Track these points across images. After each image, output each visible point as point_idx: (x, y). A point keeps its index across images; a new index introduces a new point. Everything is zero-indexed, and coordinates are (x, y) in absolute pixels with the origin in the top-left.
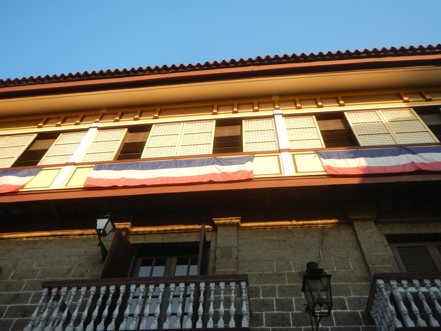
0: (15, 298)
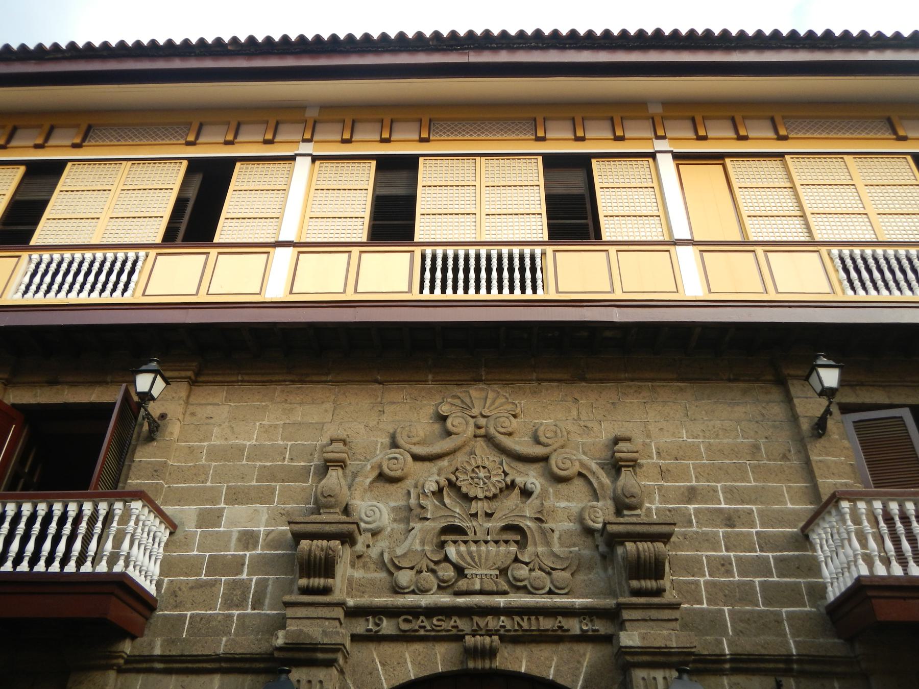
0: (691, 495)
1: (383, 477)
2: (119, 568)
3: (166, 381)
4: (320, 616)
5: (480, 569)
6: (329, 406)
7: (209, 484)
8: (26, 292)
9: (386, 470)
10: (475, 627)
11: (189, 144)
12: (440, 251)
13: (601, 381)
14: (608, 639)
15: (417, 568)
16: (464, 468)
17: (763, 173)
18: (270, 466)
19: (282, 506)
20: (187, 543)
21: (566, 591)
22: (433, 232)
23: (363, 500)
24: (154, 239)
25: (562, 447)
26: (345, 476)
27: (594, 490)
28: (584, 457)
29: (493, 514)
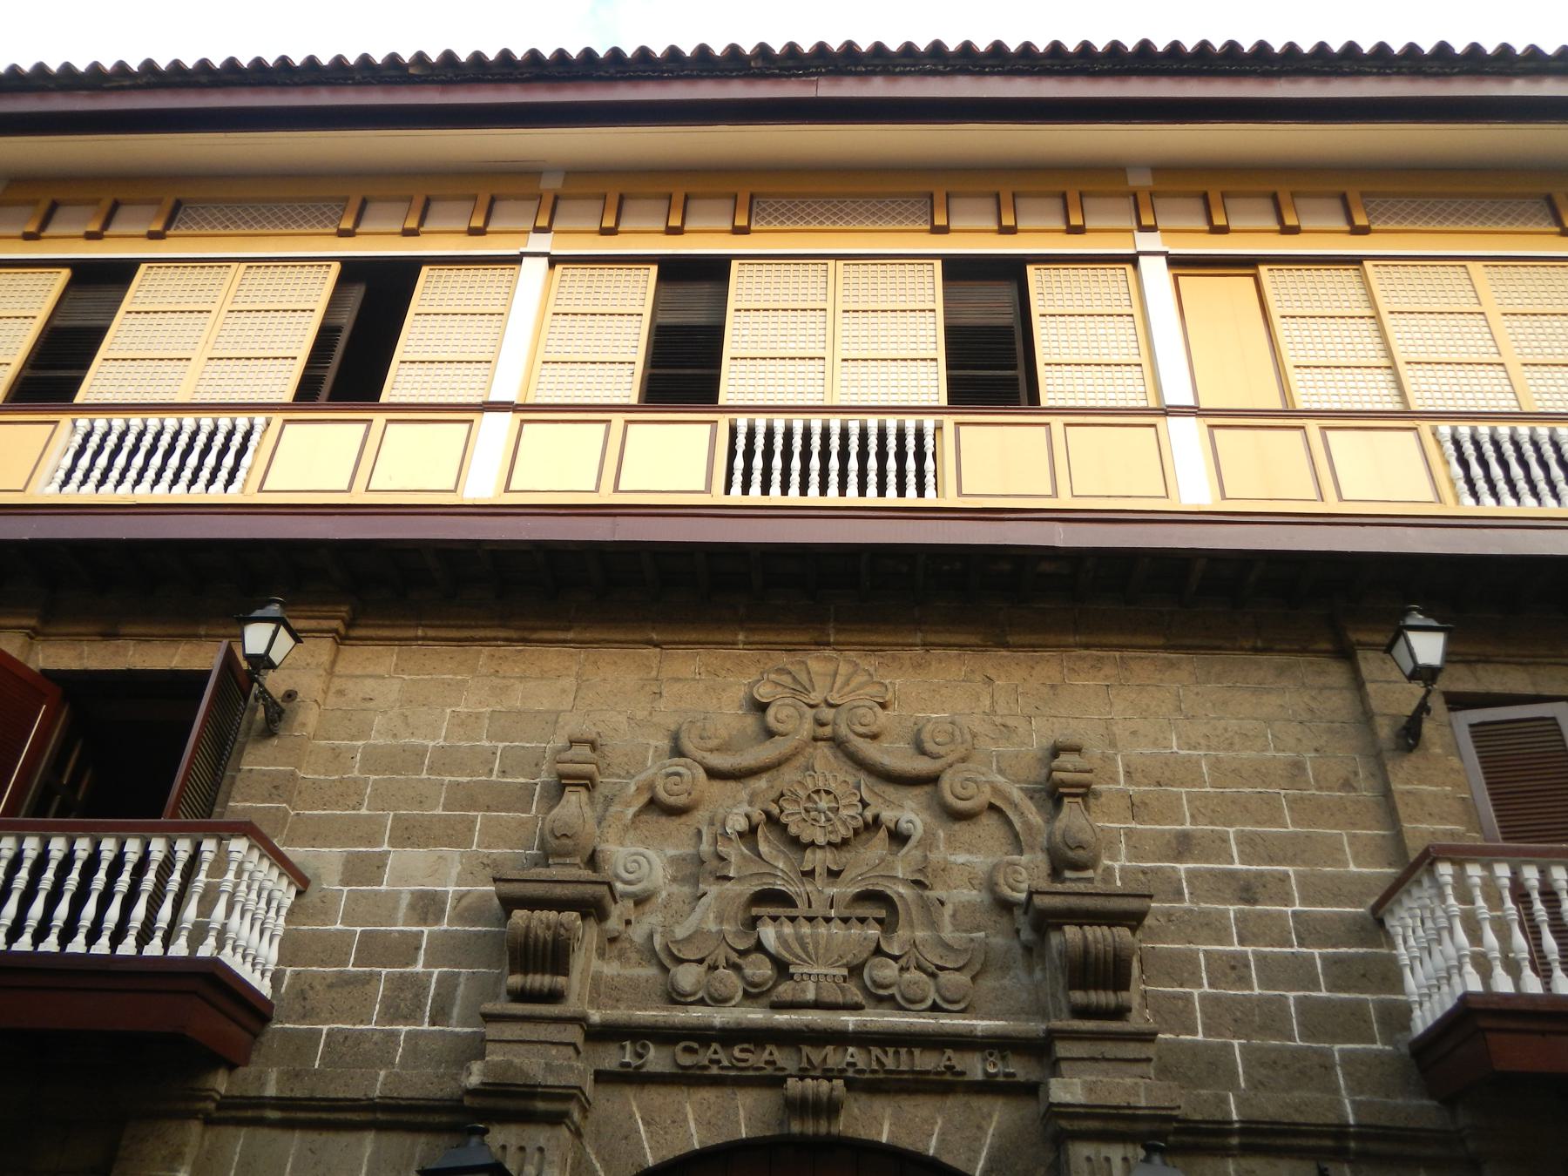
0: (1183, 846)
1: (655, 806)
2: (206, 950)
3: (296, 636)
4: (542, 1039)
5: (816, 966)
6: (569, 683)
8: (65, 483)
9: (662, 795)
10: (804, 1064)
11: (343, 234)
12: (761, 422)
13: (1033, 647)
14: (1031, 1090)
15: (708, 962)
16: (793, 793)
17: (1323, 291)
18: (468, 783)
19: (485, 851)
20: (325, 911)
21: (962, 1006)
22: (751, 389)
23: (622, 844)
24: (281, 395)
25: (963, 760)
26: (592, 801)
27: (1016, 836)
28: (1000, 779)
29: (842, 871)
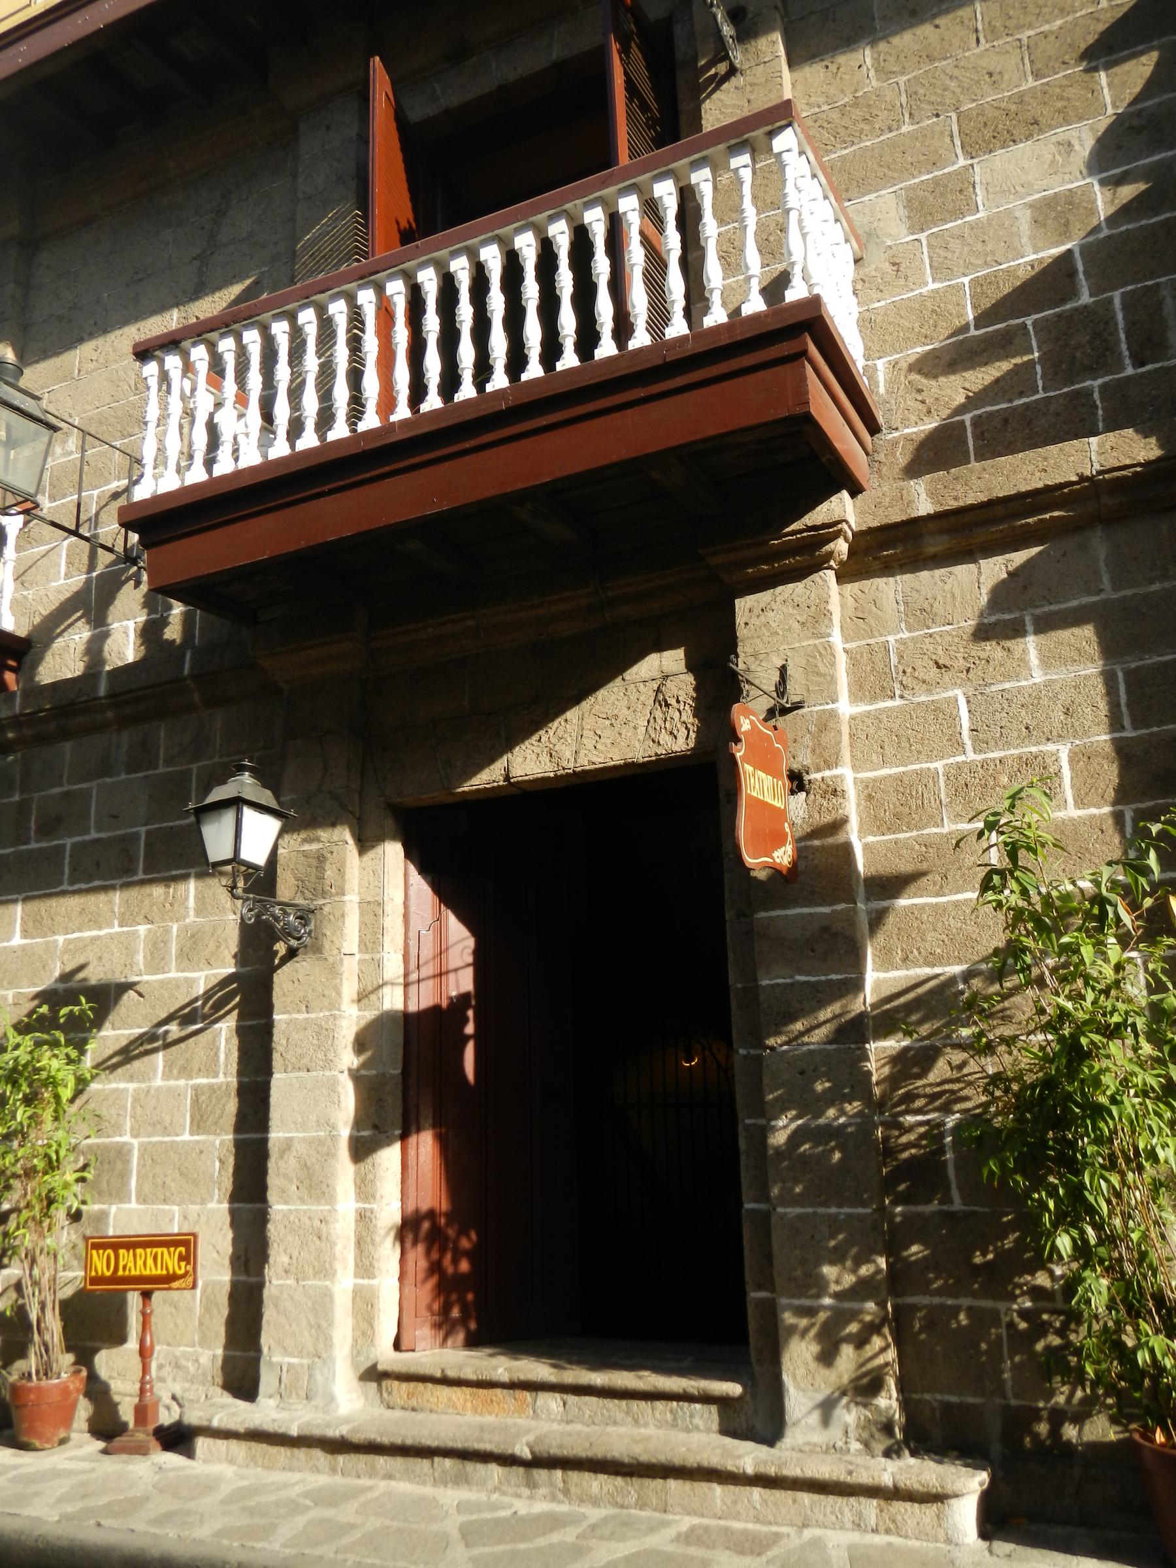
7: (905, 129)
